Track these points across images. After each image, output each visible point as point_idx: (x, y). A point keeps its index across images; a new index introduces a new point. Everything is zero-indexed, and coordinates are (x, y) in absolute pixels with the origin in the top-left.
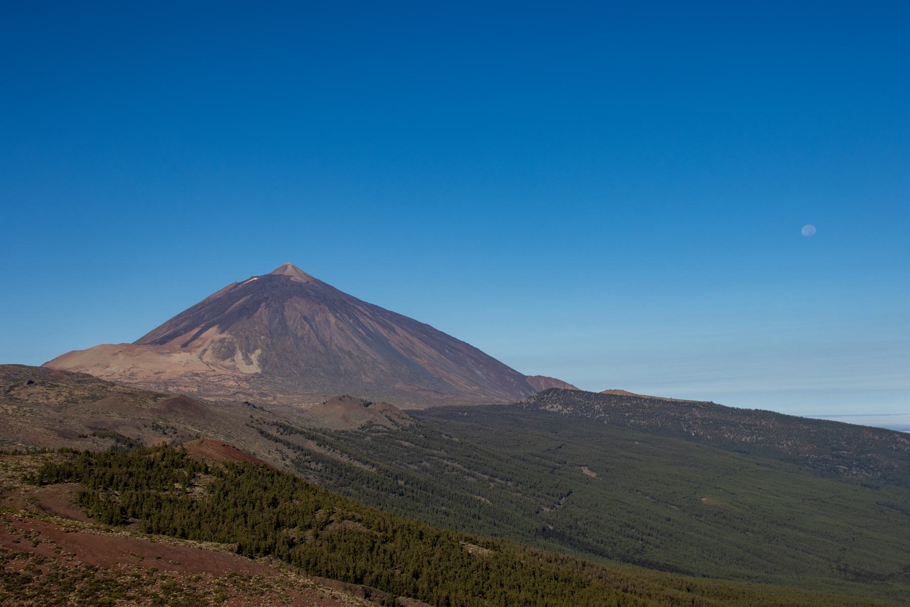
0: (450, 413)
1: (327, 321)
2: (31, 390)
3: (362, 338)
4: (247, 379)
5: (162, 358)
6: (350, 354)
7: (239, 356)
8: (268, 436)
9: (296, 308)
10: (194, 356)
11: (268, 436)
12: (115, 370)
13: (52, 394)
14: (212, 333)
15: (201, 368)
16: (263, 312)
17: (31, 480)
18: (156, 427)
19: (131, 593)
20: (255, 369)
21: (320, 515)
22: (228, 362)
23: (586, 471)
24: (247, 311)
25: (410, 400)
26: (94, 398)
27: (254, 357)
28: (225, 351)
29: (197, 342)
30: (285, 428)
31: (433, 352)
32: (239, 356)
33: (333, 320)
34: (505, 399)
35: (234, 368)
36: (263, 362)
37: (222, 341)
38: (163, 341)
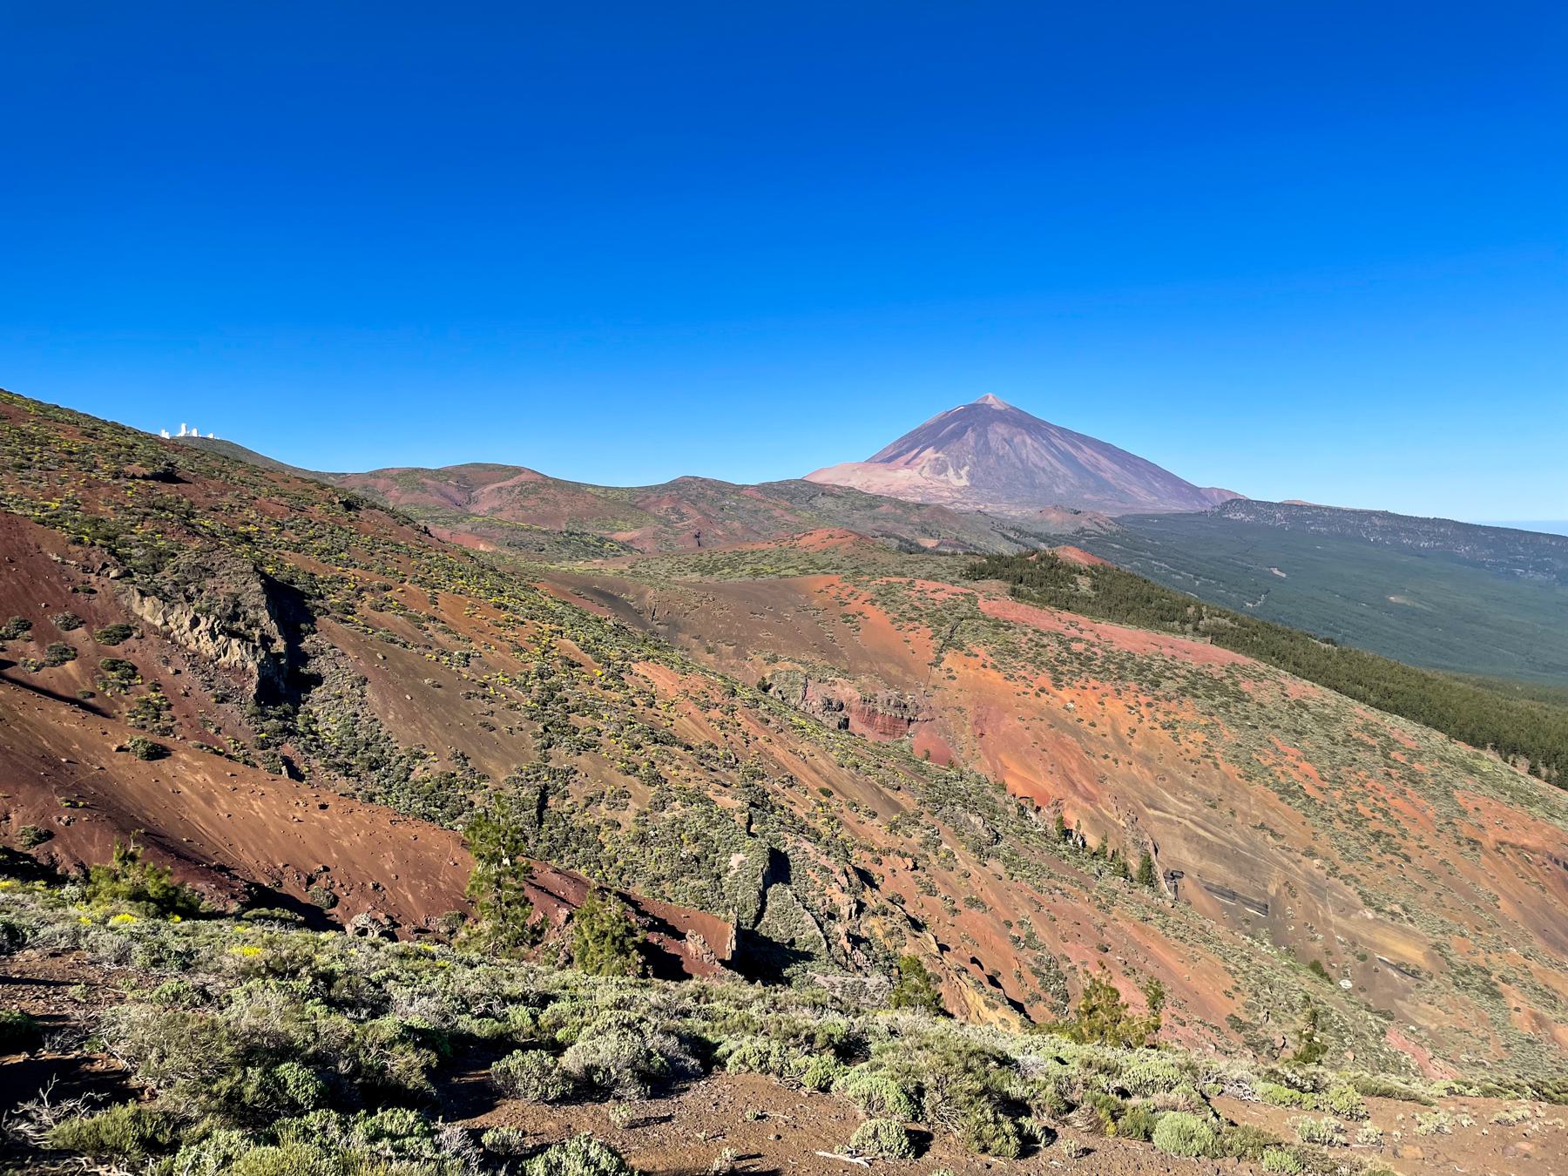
0: (1142, 519)
1: (1024, 442)
2: (824, 500)
3: (1054, 456)
4: (958, 491)
5: (891, 474)
6: (1044, 470)
7: (951, 472)
8: (1009, 538)
9: (999, 431)
10: (915, 473)
11: (1009, 538)
12: (856, 482)
13: (840, 502)
14: (929, 453)
15: (921, 482)
16: (970, 436)
17: (967, 577)
18: (924, 531)
19: (1168, 674)
20: (964, 482)
21: (1190, 610)
22: (942, 477)
23: (1276, 572)
24: (958, 434)
25: (1105, 511)
26: (872, 507)
27: (963, 473)
28: (944, 470)
29: (917, 461)
30: (1021, 532)
31: (1116, 468)
32: (951, 472)
33: (1029, 441)
34: (1196, 507)
35: (948, 482)
36: (971, 476)
37: (937, 459)
38: (890, 460)
